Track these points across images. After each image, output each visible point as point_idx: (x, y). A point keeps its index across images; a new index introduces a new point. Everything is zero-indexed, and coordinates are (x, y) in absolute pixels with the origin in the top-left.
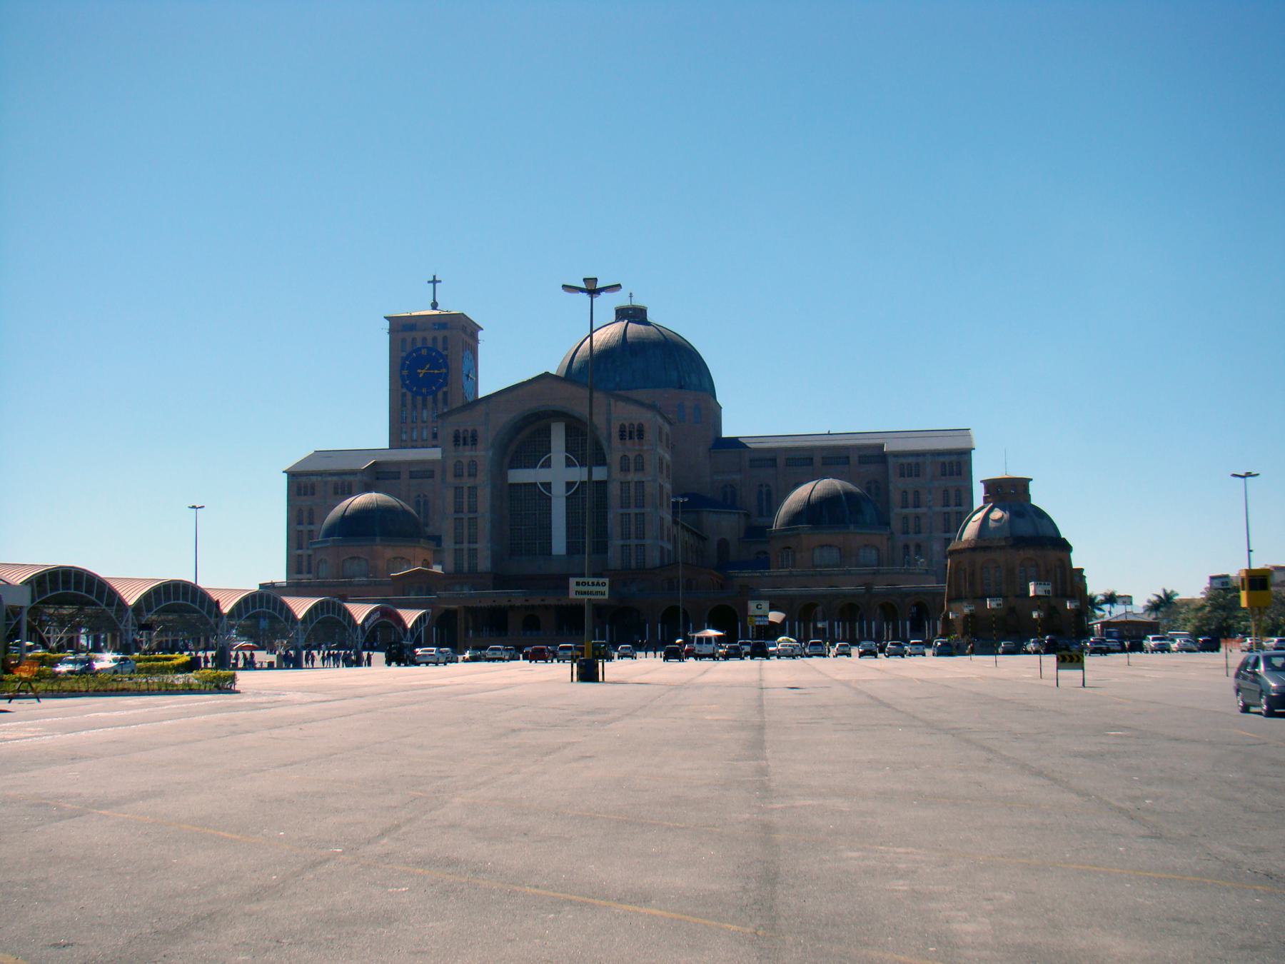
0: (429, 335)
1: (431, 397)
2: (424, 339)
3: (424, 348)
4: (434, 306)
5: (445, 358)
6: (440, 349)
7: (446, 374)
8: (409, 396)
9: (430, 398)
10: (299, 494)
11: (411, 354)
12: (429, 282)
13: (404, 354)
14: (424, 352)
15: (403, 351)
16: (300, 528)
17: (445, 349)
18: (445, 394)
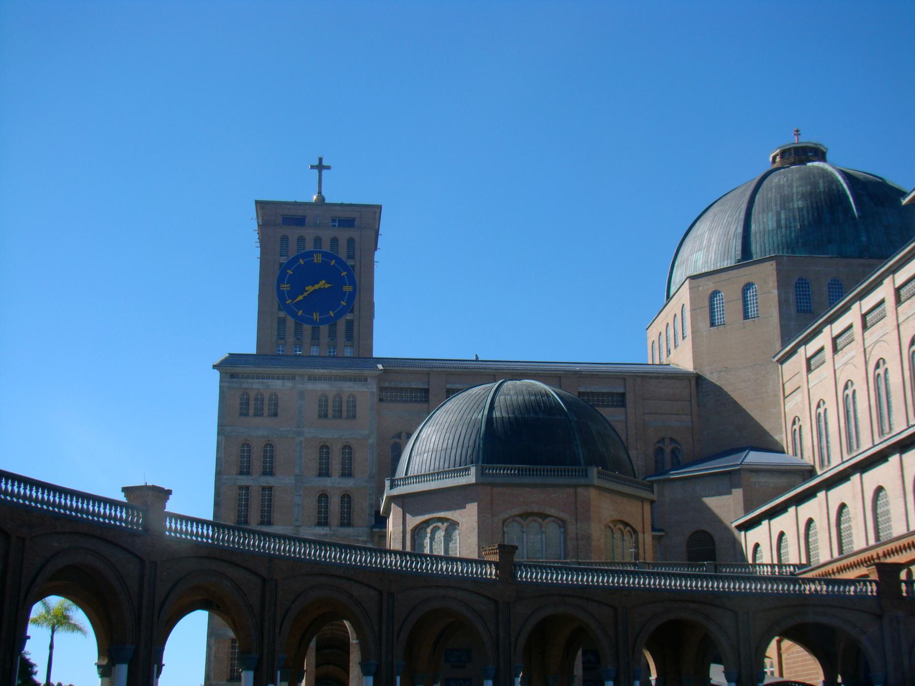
0: (326, 235)
1: (327, 326)
2: (318, 240)
3: (317, 252)
4: (321, 198)
5: (351, 270)
6: (343, 254)
7: (352, 295)
8: (291, 322)
9: (324, 329)
10: (244, 413)
11: (296, 259)
12: (312, 167)
13: (284, 260)
14: (318, 259)
15: (281, 256)
16: (244, 481)
17: (351, 256)
18: (350, 324)
